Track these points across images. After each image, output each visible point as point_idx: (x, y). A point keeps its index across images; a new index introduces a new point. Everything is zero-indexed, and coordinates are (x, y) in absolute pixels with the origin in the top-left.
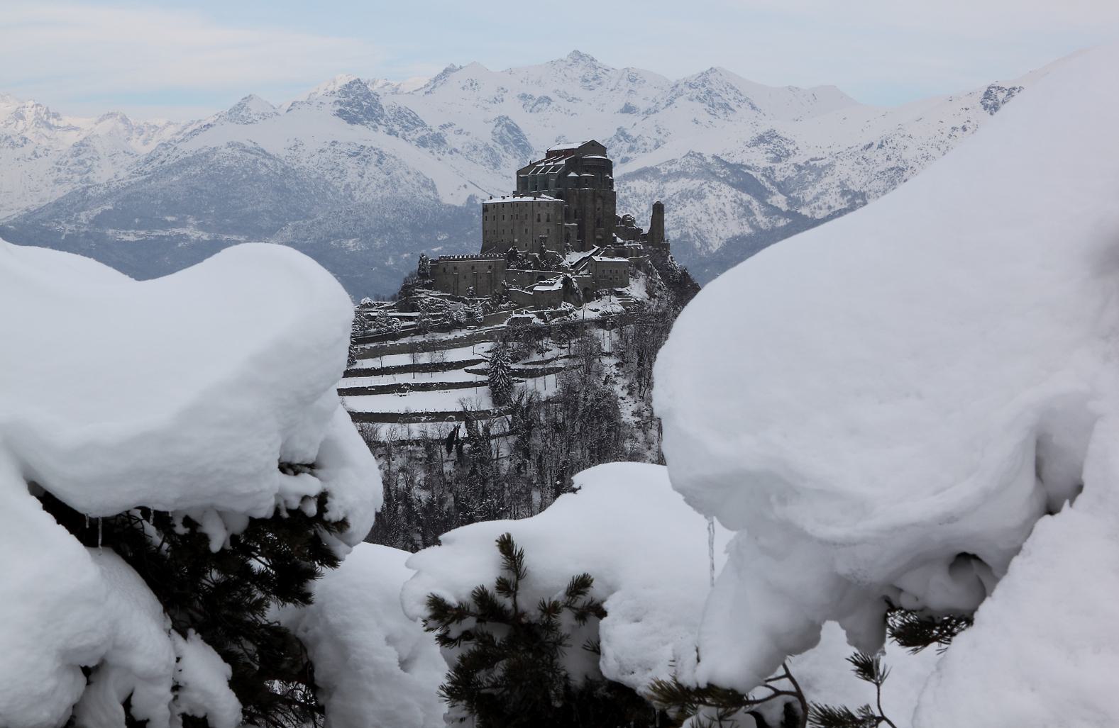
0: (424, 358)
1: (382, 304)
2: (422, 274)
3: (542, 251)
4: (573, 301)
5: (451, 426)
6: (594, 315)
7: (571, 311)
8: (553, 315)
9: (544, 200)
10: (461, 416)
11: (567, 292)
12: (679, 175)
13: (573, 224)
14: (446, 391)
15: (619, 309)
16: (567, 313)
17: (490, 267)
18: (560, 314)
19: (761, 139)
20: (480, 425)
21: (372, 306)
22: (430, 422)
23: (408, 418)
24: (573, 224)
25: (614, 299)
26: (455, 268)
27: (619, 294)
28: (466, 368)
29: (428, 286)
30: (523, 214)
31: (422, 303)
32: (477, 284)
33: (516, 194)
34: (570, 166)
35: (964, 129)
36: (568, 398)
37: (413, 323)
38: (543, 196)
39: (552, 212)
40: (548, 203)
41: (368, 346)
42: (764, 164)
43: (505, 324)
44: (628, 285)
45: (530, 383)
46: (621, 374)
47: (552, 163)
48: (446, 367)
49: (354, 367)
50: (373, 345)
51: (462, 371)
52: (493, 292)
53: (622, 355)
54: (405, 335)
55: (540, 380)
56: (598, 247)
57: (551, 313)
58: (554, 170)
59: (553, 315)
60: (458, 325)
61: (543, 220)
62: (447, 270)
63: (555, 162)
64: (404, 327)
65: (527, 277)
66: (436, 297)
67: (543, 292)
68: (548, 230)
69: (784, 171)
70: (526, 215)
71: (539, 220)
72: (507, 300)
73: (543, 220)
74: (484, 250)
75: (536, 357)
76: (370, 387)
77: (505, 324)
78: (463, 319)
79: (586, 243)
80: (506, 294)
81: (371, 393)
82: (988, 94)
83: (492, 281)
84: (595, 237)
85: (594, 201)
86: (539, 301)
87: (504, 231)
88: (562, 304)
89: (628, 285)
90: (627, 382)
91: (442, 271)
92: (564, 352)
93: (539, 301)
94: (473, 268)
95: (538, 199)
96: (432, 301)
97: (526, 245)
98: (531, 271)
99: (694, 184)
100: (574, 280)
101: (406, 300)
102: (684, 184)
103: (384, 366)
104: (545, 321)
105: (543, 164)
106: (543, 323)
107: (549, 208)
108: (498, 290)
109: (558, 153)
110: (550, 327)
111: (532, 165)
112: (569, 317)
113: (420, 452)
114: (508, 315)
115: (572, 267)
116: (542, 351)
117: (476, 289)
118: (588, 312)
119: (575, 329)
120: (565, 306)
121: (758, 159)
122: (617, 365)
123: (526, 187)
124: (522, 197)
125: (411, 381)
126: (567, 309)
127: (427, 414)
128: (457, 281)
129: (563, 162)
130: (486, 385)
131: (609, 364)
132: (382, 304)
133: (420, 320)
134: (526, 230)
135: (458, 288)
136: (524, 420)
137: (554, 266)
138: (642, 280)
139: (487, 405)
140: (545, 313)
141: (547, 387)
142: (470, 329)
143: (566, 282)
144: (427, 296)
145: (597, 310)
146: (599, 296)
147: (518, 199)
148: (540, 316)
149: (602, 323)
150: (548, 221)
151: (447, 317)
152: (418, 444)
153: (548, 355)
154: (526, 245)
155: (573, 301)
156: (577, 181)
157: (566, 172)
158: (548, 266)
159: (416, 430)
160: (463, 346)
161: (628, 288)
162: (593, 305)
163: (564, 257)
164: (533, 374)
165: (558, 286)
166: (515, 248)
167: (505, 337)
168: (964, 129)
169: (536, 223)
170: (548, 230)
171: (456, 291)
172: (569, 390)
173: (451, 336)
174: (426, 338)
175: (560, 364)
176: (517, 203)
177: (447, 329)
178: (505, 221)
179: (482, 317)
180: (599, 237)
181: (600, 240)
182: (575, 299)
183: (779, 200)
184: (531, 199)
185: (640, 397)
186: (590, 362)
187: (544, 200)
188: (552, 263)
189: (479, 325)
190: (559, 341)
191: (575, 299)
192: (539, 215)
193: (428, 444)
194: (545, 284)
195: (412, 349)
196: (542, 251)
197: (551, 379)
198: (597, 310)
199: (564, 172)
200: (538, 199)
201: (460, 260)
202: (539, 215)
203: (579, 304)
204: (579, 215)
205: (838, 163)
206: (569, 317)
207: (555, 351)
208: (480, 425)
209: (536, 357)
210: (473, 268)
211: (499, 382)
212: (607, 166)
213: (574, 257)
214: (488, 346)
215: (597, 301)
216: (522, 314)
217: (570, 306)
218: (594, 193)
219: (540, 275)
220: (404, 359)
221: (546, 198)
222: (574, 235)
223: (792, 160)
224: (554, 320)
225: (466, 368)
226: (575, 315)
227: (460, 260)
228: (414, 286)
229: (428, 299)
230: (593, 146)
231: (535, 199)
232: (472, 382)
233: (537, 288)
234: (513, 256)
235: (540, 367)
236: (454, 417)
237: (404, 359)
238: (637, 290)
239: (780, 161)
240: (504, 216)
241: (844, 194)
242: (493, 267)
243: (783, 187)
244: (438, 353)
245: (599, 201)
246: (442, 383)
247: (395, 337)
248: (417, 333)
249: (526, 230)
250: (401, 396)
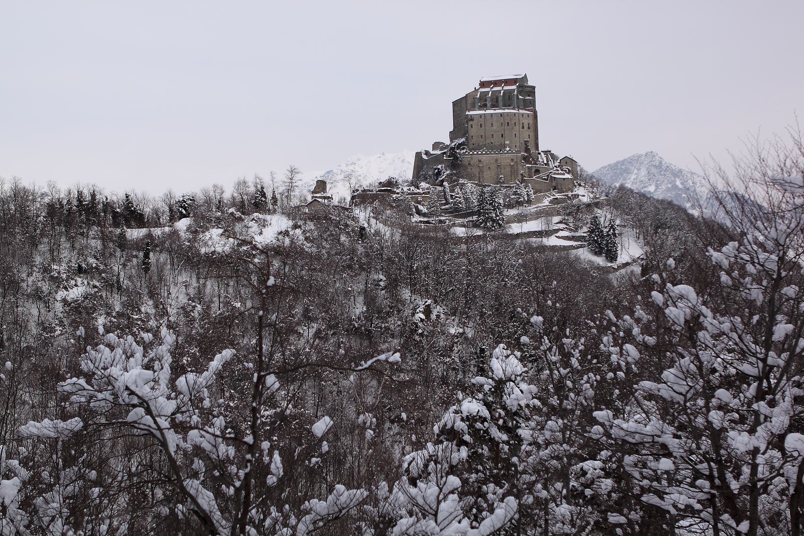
3: (527, 150)
26: (480, 161)
43: (546, 202)
61: (526, 128)
67: (564, 179)
71: (523, 128)
73: (526, 128)
77: (546, 202)
94: (496, 160)
109: (496, 83)
111: (476, 90)
128: (481, 171)
129: (514, 87)
150: (529, 128)
169: (521, 130)
171: (481, 180)
178: (495, 127)
210: (496, 160)
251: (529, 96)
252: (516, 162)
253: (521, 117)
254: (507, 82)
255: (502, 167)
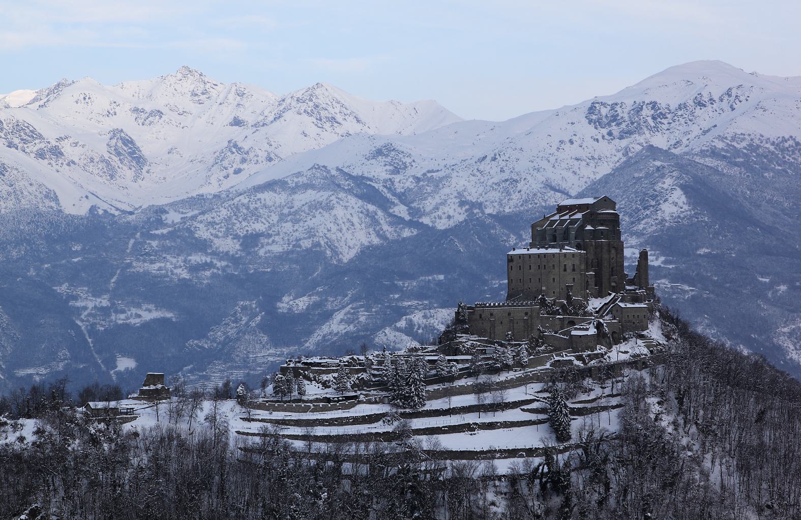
0: (488, 398)
1: (426, 348)
2: (459, 320)
3: (569, 298)
4: (604, 343)
5: (537, 461)
6: (623, 357)
7: (606, 353)
8: (591, 357)
9: (569, 251)
10: (530, 452)
11: (601, 336)
12: (307, 187)
13: (591, 273)
14: (509, 429)
15: (645, 351)
16: (602, 355)
17: (526, 314)
18: (597, 356)
19: (379, 152)
20: (561, 459)
21: (416, 350)
22: (503, 458)
23: (490, 454)
24: (591, 273)
25: (640, 342)
26: (492, 314)
27: (642, 337)
28: (522, 407)
29: (466, 331)
30: (551, 265)
31: (464, 346)
32: (513, 329)
33: (532, 245)
34: (587, 220)
35: (571, 142)
36: (627, 435)
37: (467, 365)
38: (566, 247)
39: (577, 262)
40: (573, 255)
41: (431, 388)
42: (384, 176)
43: (548, 366)
44: (647, 328)
45: (588, 419)
46: (664, 411)
47: (567, 217)
48: (504, 407)
49: (425, 408)
50: (436, 387)
51: (518, 410)
52: (530, 336)
53: (662, 394)
54: (460, 377)
55: (595, 416)
56: (614, 294)
57: (589, 356)
58: (570, 223)
59: (591, 357)
60: (507, 368)
61: (569, 270)
62: (483, 316)
63: (570, 216)
64: (461, 370)
65: (558, 322)
66: (474, 341)
67: (580, 336)
68: (574, 279)
69: (403, 182)
70: (554, 265)
71: (565, 270)
72: (543, 344)
73: (569, 270)
74: (509, 297)
75: (584, 397)
76: (444, 427)
77: (548, 366)
78: (511, 362)
79: (603, 290)
80: (541, 338)
81: (445, 432)
82: (592, 109)
83: (528, 326)
84: (610, 284)
85: (609, 251)
86: (574, 344)
87: (530, 279)
88: (598, 348)
89: (647, 328)
90: (671, 418)
91: (478, 317)
92: (607, 391)
93: (574, 344)
94: (509, 314)
95: (564, 251)
96: (472, 345)
97: (554, 292)
98: (562, 317)
99: (322, 196)
100: (605, 325)
101: (447, 342)
102: (310, 195)
103: (536, 415)
104: (584, 362)
105: (557, 217)
106: (582, 365)
107: (573, 259)
108: (535, 334)
109: (571, 208)
110: (590, 369)
112: (605, 359)
113: (503, 485)
114: (549, 358)
115: (597, 312)
116: (588, 391)
117: (513, 335)
118: (617, 354)
119: (613, 370)
120: (600, 349)
121: (378, 171)
122: (659, 403)
123: (544, 238)
124: (547, 249)
125: (479, 421)
126: (602, 351)
127: (500, 451)
128: (493, 326)
129: (579, 216)
130: (546, 422)
131: (652, 400)
132: (426, 348)
133: (474, 363)
134: (554, 279)
135: (494, 333)
136: (593, 455)
137: (581, 312)
138: (657, 323)
139: (552, 443)
140: (584, 356)
141: (609, 423)
142: (516, 371)
143: (599, 326)
144: (467, 340)
145: (626, 352)
146: (625, 339)
147: (534, 251)
148: (579, 358)
149: (636, 363)
150: (574, 270)
151: (498, 360)
152: (500, 480)
153: (592, 396)
154: (554, 292)
155: (604, 343)
156: (595, 234)
157: (582, 227)
158: (574, 312)
159: (503, 466)
160: (514, 387)
161: (648, 331)
162: (623, 347)
163: (588, 303)
164: (580, 412)
165: (592, 331)
166: (543, 296)
167: (550, 378)
168: (571, 142)
169: (562, 272)
170: (574, 279)
171: (492, 336)
172: (626, 427)
173: (503, 377)
174: (482, 379)
175: (614, 401)
176: (545, 255)
177: (497, 371)
178: (532, 271)
179: (527, 360)
180: (613, 284)
181: (614, 287)
182: (607, 342)
183: (401, 210)
184: (556, 251)
185: (685, 433)
186: (637, 400)
187: (569, 251)
188: (579, 309)
189: (523, 367)
190: (601, 382)
191: (607, 342)
192: (565, 265)
193: (513, 479)
194: (580, 329)
195: (479, 389)
196: (569, 298)
197: (604, 415)
198: (626, 352)
199: (582, 225)
200: (564, 251)
201: (496, 307)
202: (565, 265)
203: (610, 347)
204: (598, 266)
205: (454, 174)
206: (605, 359)
207: (597, 391)
208: (561, 459)
209: (584, 397)
210: (509, 314)
211: (564, 421)
212: (614, 220)
213: (595, 304)
214: (538, 386)
215: (624, 343)
216: (563, 356)
217: (604, 349)
218: (609, 244)
219: (570, 320)
220: (469, 400)
221: (569, 250)
222: (592, 282)
223: (410, 172)
224: (592, 362)
225: (522, 407)
226: (609, 357)
227: (496, 307)
228: (456, 331)
229: (469, 343)
230: (607, 202)
231: (561, 251)
232: (531, 420)
233: (574, 333)
234: (543, 302)
235: (589, 406)
236: (524, 453)
237: (469, 400)
238: (655, 332)
239: (398, 173)
240: (530, 266)
241: (462, 204)
242: (529, 314)
243: (403, 198)
244: (498, 393)
245: (613, 251)
246: (505, 422)
247: (452, 379)
248: (469, 375)
249: (554, 279)
250: (471, 434)
251: (602, 225)
252: (531, 316)
253: (562, 258)
254: (580, 208)
255: (515, 321)
